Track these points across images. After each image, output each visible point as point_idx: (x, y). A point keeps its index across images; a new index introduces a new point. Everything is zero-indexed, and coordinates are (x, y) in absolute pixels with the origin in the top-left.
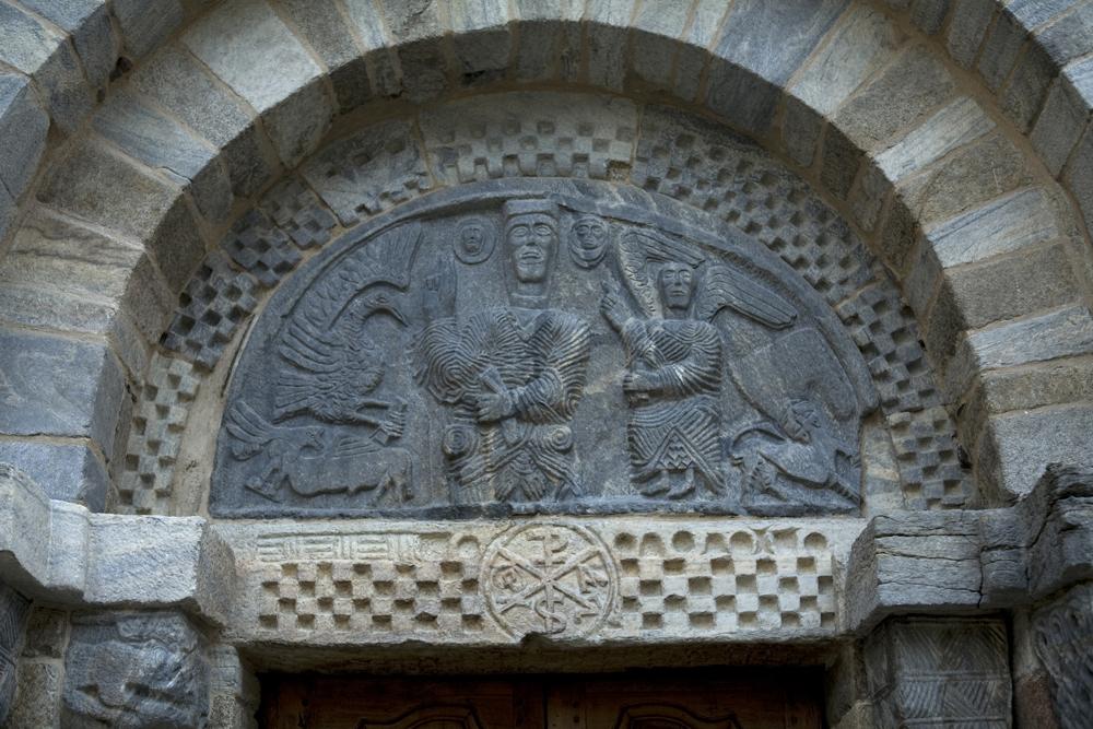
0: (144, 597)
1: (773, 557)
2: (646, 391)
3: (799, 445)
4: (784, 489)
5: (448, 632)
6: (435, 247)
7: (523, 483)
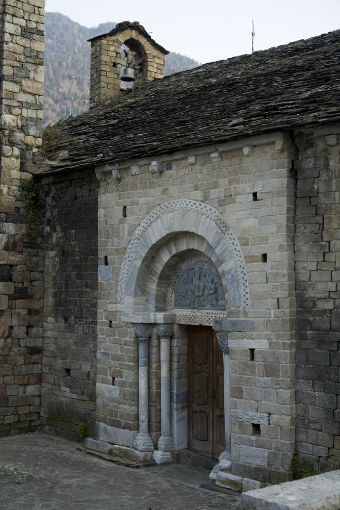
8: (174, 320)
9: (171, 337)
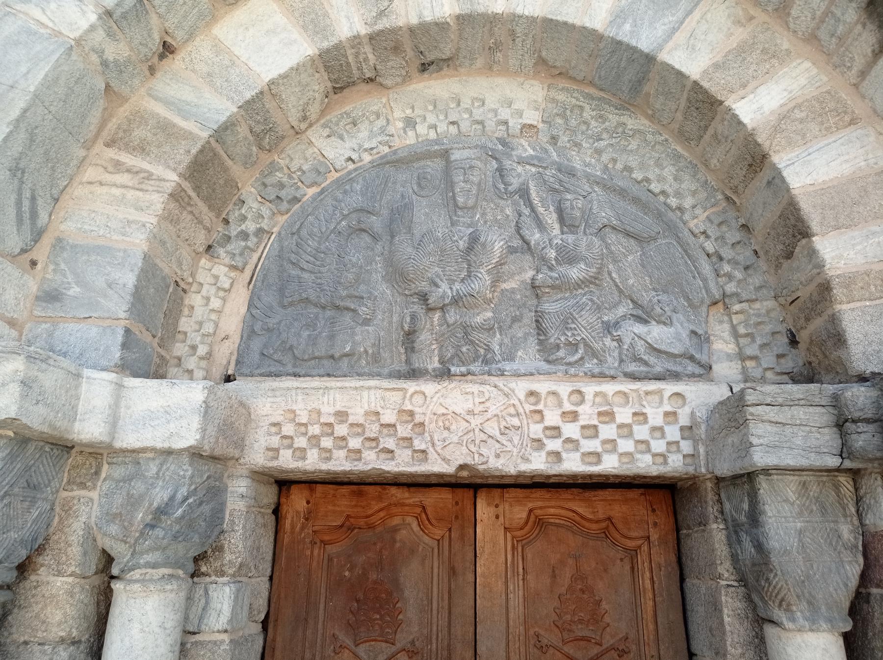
0: (159, 445)
1: (644, 411)
2: (549, 286)
3: (662, 326)
4: (652, 360)
5: (402, 464)
6: (398, 186)
7: (459, 352)
8: (240, 444)
9: (198, 566)
